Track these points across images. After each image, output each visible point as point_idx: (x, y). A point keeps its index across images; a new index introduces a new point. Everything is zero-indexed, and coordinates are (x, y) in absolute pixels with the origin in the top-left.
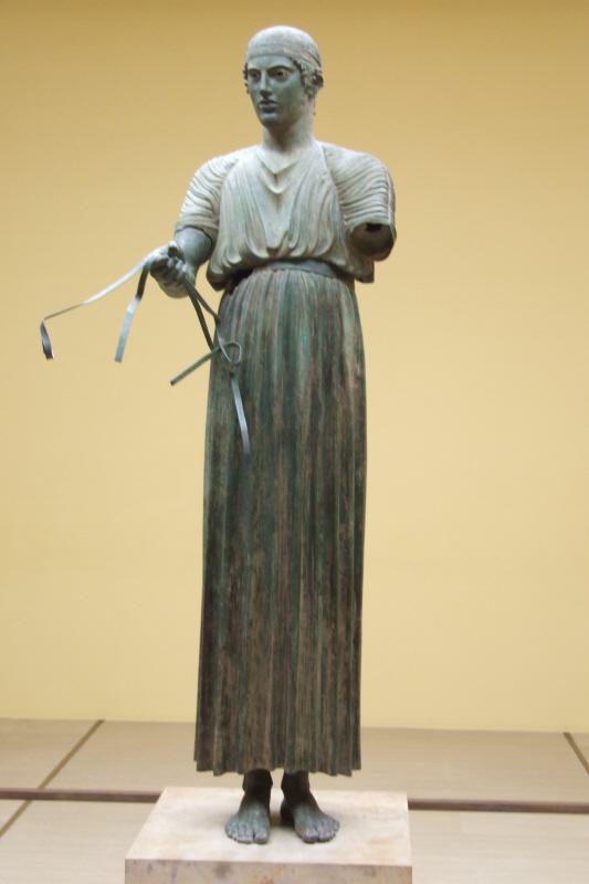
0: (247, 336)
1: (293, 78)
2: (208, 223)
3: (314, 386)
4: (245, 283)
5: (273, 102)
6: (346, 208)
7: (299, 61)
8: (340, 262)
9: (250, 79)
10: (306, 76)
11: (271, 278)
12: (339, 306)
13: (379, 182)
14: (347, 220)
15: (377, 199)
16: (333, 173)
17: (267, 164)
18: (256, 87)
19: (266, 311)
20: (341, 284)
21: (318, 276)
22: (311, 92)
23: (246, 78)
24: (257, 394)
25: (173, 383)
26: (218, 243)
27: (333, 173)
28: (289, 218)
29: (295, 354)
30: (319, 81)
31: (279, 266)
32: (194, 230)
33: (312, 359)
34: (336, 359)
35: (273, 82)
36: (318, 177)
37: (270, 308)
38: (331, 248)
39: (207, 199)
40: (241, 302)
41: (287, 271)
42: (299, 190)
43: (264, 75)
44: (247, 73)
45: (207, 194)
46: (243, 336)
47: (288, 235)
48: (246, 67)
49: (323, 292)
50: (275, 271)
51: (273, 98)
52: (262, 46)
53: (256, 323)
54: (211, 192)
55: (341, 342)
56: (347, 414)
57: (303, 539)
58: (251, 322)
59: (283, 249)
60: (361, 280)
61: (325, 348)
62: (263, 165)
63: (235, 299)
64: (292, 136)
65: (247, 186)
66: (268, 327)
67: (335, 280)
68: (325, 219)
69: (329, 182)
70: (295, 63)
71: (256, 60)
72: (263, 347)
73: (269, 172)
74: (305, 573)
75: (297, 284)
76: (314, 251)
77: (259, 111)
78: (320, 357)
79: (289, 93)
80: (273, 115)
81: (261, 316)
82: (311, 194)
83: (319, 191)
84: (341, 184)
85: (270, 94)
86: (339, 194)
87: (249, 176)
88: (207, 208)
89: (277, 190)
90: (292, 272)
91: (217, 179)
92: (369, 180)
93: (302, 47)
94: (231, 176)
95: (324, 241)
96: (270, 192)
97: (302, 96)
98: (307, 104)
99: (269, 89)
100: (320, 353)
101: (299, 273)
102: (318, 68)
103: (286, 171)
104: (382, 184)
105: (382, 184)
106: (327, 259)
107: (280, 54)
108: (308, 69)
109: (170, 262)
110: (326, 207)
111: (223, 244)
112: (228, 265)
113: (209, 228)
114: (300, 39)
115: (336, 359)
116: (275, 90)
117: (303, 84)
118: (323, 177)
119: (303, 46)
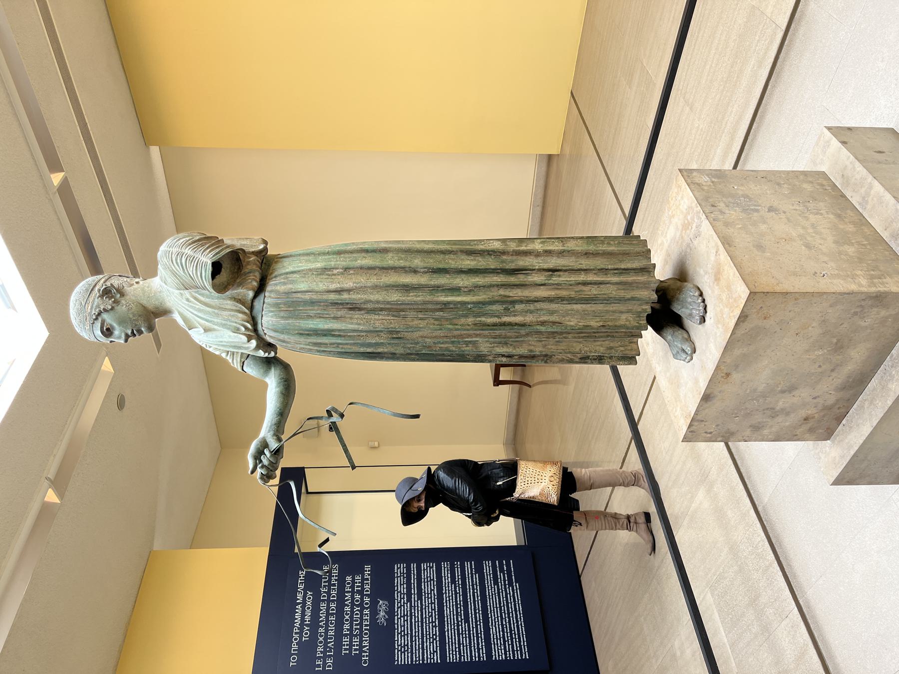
8: (251, 294)
20: (269, 288)
24: (362, 350)
31: (261, 332)
47: (237, 331)
49: (277, 305)
51: (129, 332)
56: (375, 287)
57: (470, 320)
67: (267, 294)
69: (187, 294)
70: (96, 319)
74: (498, 317)
79: (122, 322)
82: (200, 310)
93: (81, 310)
97: (122, 309)
99: (123, 336)
108: (98, 306)
113: (241, 357)
116: (121, 331)
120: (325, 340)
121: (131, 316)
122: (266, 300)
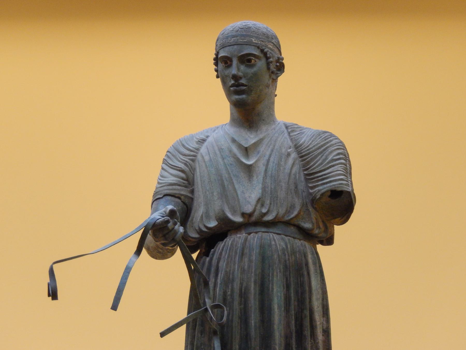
0: (225, 293)
1: (261, 64)
2: (184, 192)
3: (287, 337)
4: (221, 245)
5: (243, 85)
6: (310, 176)
7: (265, 50)
8: (307, 225)
9: (221, 65)
10: (271, 62)
11: (246, 239)
12: (307, 264)
13: (339, 154)
14: (312, 188)
15: (339, 169)
16: (297, 147)
17: (236, 138)
18: (227, 72)
19: (243, 271)
21: (287, 238)
22: (274, 76)
23: (216, 64)
25: (163, 334)
26: (193, 212)
27: (297, 147)
28: (261, 185)
29: (270, 309)
30: (281, 68)
31: (252, 229)
32: (173, 199)
33: (283, 314)
34: (307, 313)
35: (242, 67)
36: (284, 150)
37: (246, 267)
38: (299, 213)
39: (183, 171)
40: (218, 262)
41: (260, 234)
42: (268, 161)
43: (235, 62)
44: (217, 60)
45: (182, 166)
46: (222, 293)
47: (260, 201)
48: (217, 54)
49: (293, 252)
50: (249, 234)
51: (243, 81)
52: (234, 36)
53: (233, 280)
54: (185, 164)
55: (310, 299)
58: (228, 281)
59: (256, 214)
60: (322, 243)
61: (296, 303)
62: (234, 141)
63: (211, 259)
64: (259, 115)
65: (220, 160)
66: (244, 285)
68: (292, 187)
69: (294, 155)
70: (262, 51)
71: (227, 49)
72: (240, 304)
73: (240, 146)
75: (270, 245)
76: (283, 217)
77: (229, 93)
78: (293, 312)
80: (244, 96)
81: (237, 274)
82: (279, 165)
83: (285, 163)
84: (305, 156)
85: (241, 78)
86: (304, 166)
87: (221, 150)
88: (183, 179)
90: (265, 235)
91: (192, 153)
92: (331, 152)
94: (203, 150)
95: (292, 207)
96: (242, 163)
98: (271, 86)
99: (240, 74)
100: (292, 307)
101: (271, 235)
102: (279, 56)
103: (256, 145)
104: (341, 156)
105: (341, 156)
106: (296, 223)
107: (249, 44)
108: (273, 57)
109: (170, 225)
110: (293, 176)
111: (199, 212)
112: (204, 229)
113: (186, 196)
114: (265, 30)
115: (307, 313)
116: (245, 76)
117: (269, 69)
118: (289, 150)
119: (268, 37)
120: (253, 303)
121: (261, 88)
122: (297, 241)
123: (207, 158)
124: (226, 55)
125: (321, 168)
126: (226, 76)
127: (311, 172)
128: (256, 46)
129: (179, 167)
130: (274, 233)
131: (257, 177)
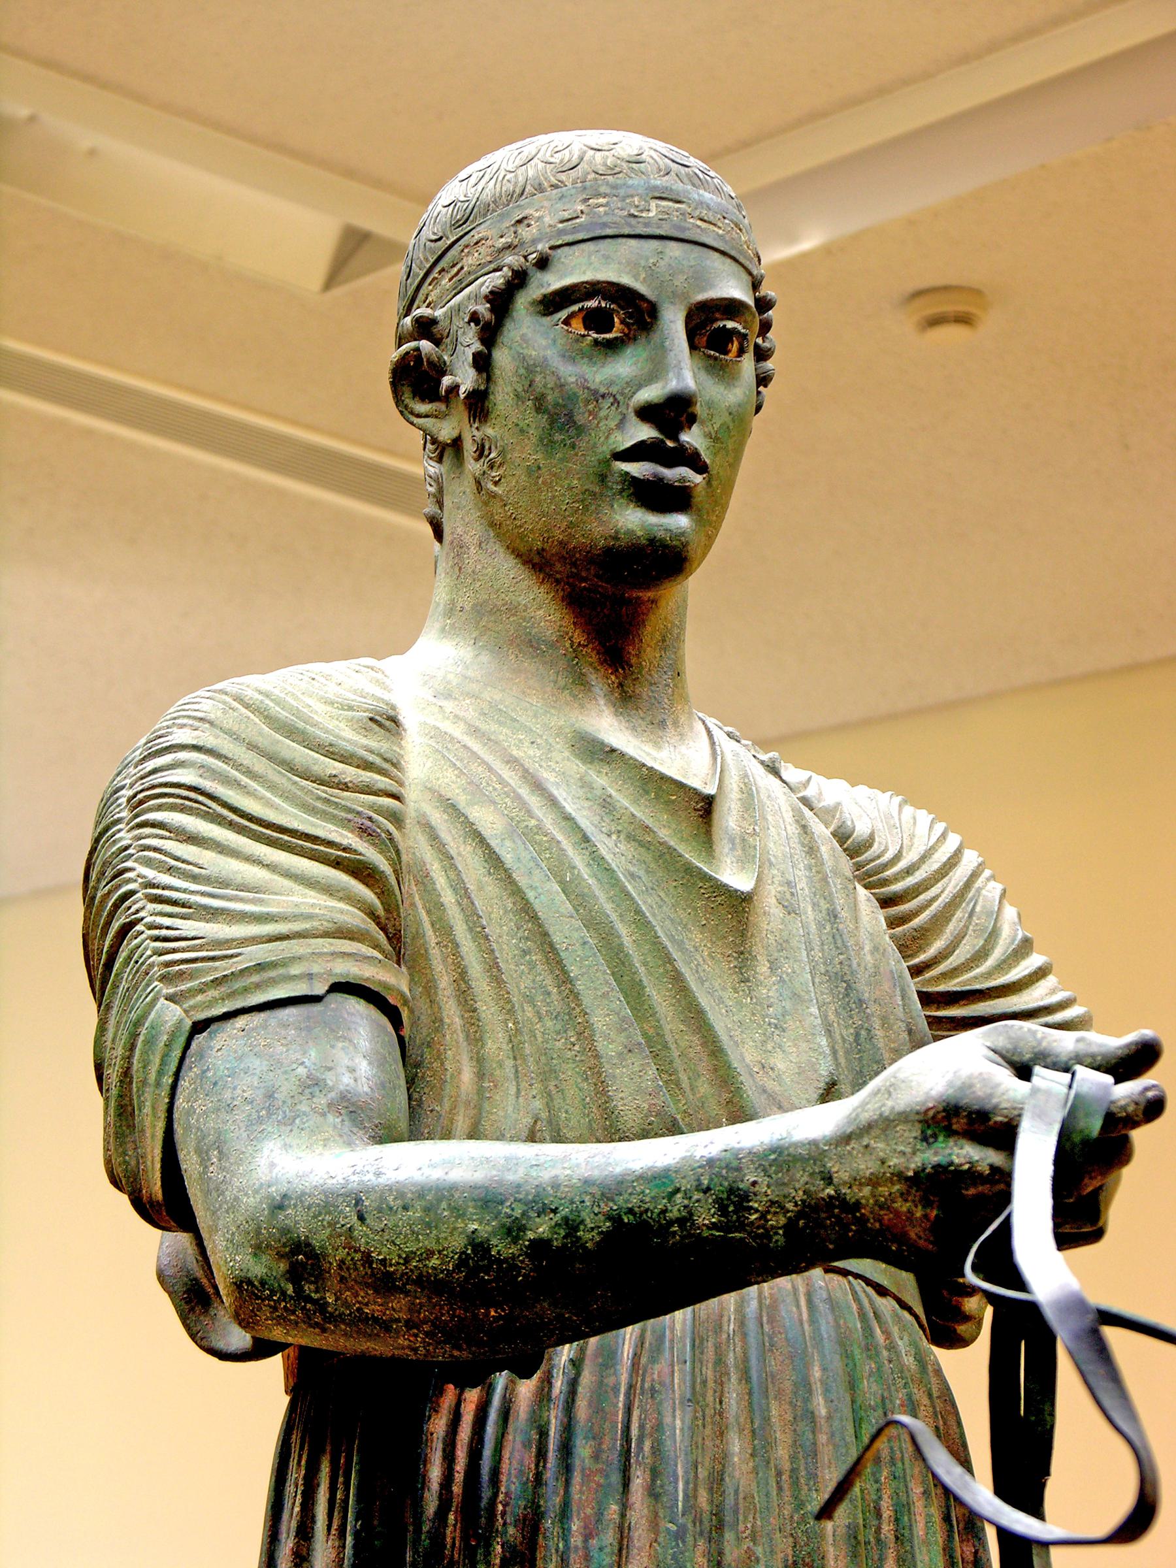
5: (694, 461)
54: (364, 832)
88: (372, 914)
89: (739, 880)
123: (487, 819)
124: (626, 280)
125: (989, 975)
126: (597, 396)
127: (942, 988)
128: (750, 273)
129: (330, 844)
130: (868, 1282)
131: (773, 966)
